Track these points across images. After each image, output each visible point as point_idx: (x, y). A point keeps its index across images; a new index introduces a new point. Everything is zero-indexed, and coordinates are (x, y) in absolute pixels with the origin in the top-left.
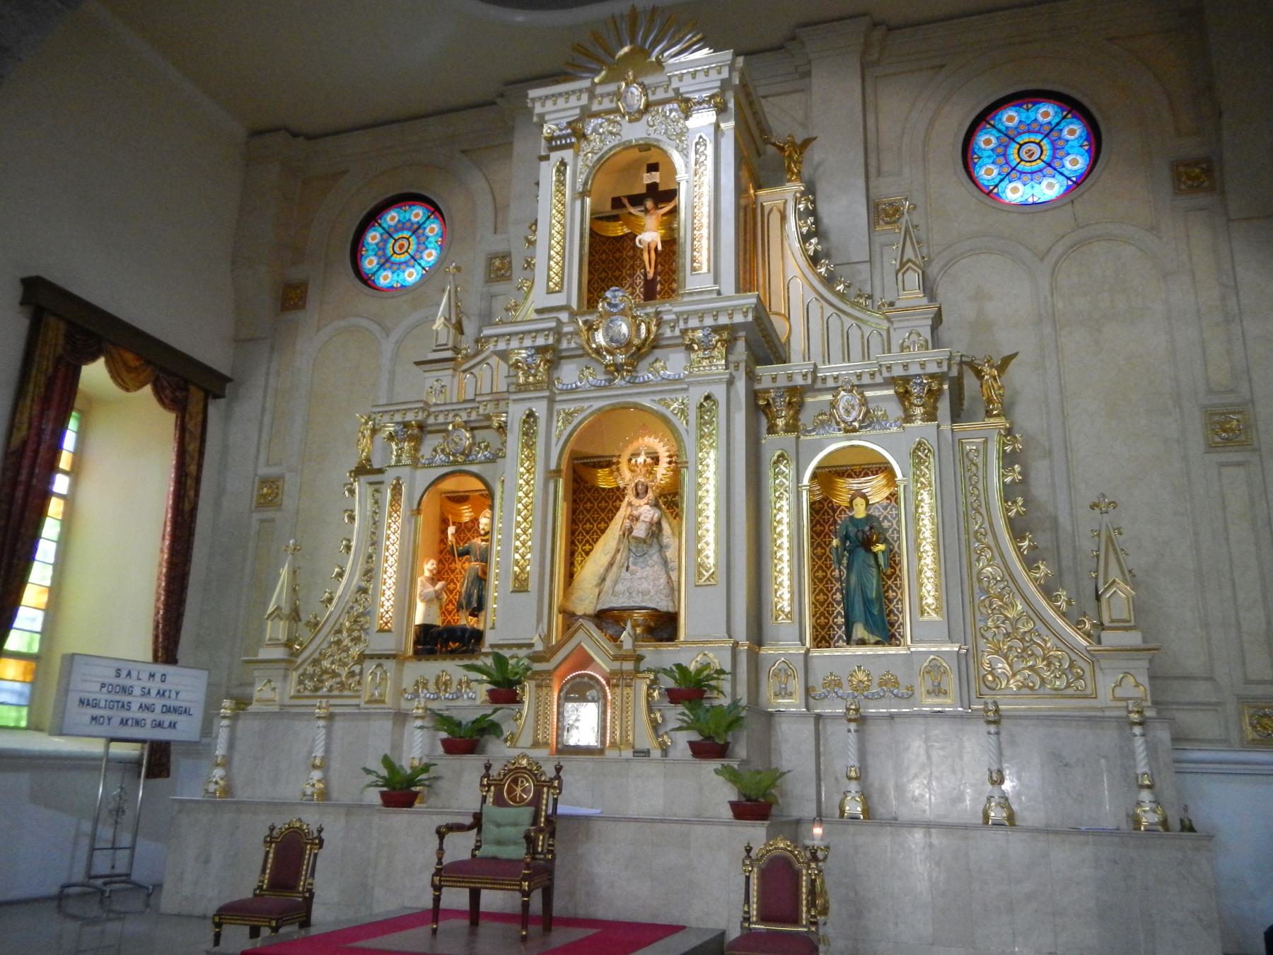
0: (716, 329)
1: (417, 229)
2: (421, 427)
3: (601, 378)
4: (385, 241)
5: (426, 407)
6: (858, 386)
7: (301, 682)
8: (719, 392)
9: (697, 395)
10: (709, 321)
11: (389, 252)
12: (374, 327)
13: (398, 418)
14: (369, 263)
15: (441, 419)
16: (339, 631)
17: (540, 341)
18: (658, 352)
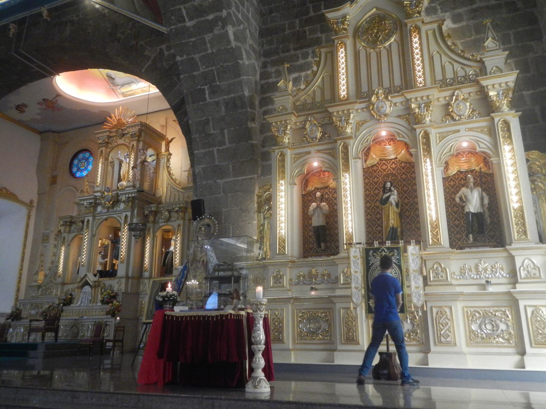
0: (129, 198)
1: (87, 159)
2: (71, 222)
3: (106, 210)
4: (78, 163)
5: (71, 217)
6: (168, 210)
7: (42, 291)
8: (129, 214)
9: (124, 214)
10: (127, 196)
11: (80, 166)
12: (75, 191)
13: (64, 220)
14: (74, 170)
15: (75, 220)
16: (51, 278)
17: (91, 201)
18: (119, 203)
